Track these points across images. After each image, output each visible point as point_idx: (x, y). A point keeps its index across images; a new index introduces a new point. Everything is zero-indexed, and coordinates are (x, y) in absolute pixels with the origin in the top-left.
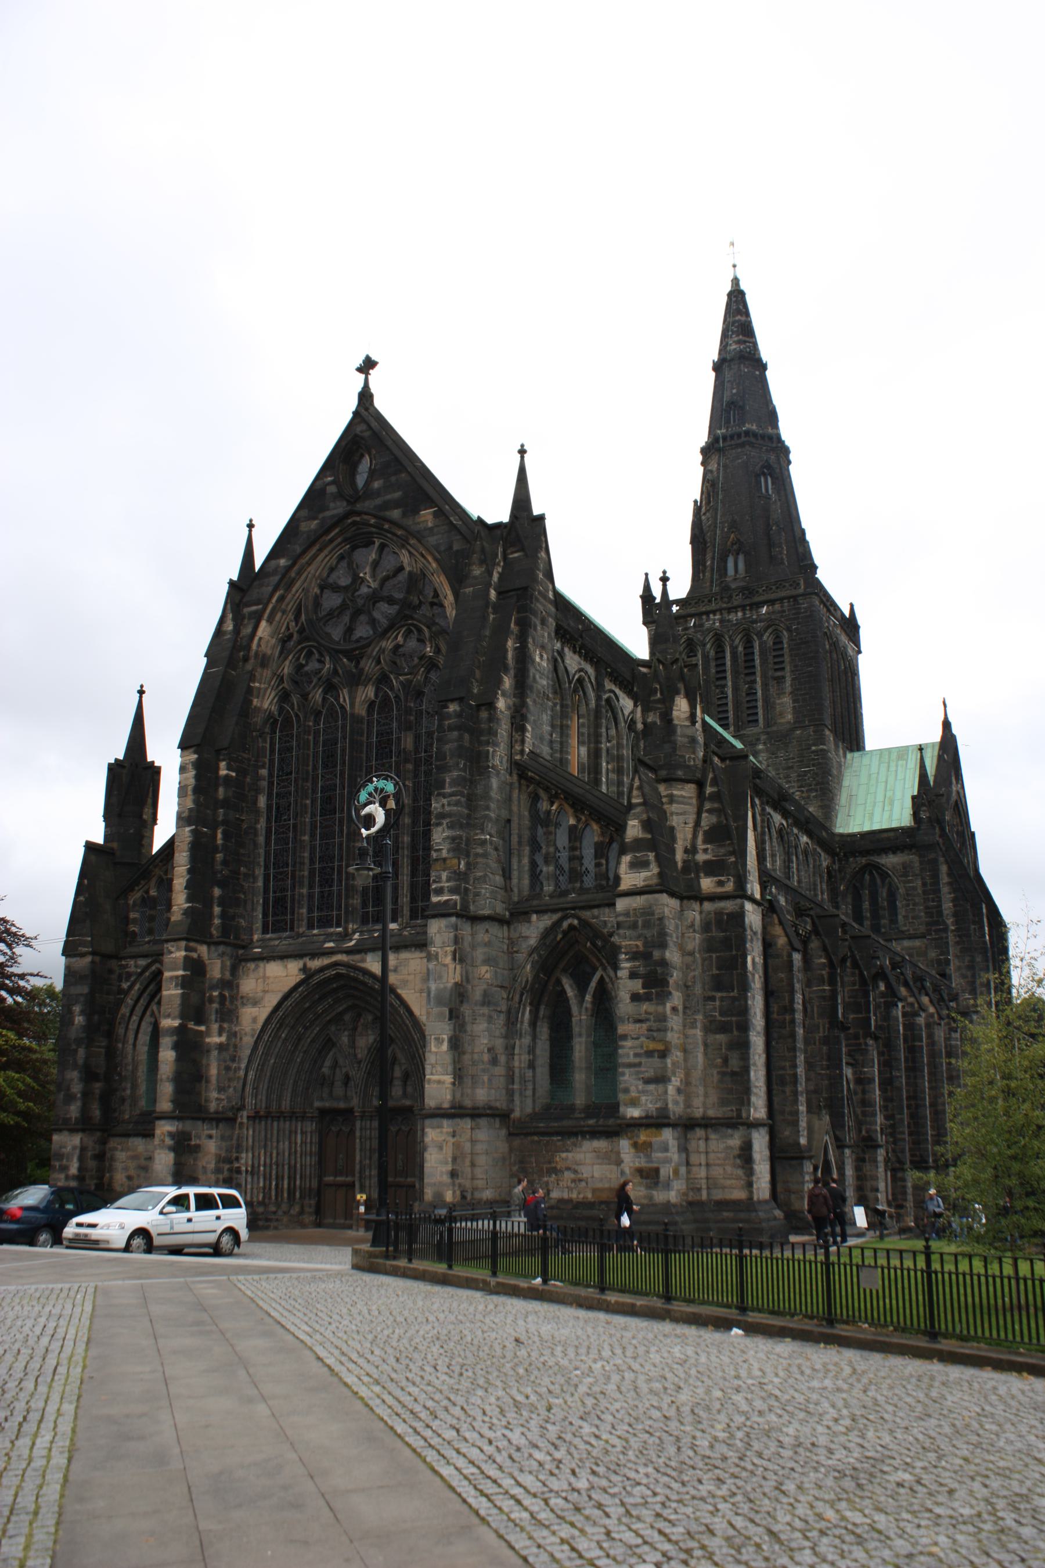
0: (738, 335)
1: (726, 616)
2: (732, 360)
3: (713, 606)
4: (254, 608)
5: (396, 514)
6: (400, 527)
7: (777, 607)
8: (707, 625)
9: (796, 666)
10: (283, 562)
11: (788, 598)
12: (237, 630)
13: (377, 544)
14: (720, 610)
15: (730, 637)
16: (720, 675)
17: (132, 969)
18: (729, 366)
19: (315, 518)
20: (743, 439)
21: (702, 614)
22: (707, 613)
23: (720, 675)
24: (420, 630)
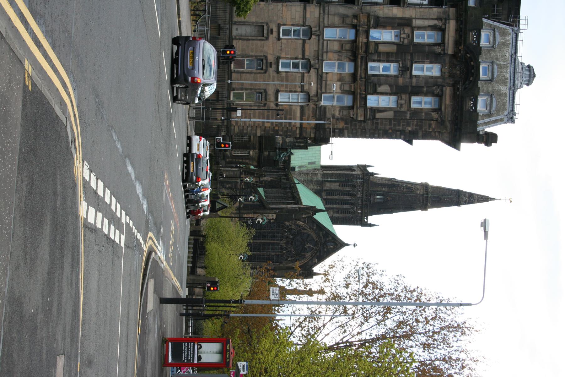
0: (469, 201)
1: (360, 199)
2: (459, 199)
3: (364, 196)
4: (307, 221)
5: (318, 254)
6: (315, 255)
7: (360, 215)
8: (359, 193)
9: (340, 219)
10: (315, 228)
11: (362, 218)
12: (303, 218)
13: (314, 247)
14: (363, 198)
15: (353, 200)
16: (343, 194)
17: (238, 192)
18: (456, 198)
19: (322, 235)
20: (425, 203)
21: (363, 192)
22: (363, 193)
23: (343, 194)
24: (294, 257)
